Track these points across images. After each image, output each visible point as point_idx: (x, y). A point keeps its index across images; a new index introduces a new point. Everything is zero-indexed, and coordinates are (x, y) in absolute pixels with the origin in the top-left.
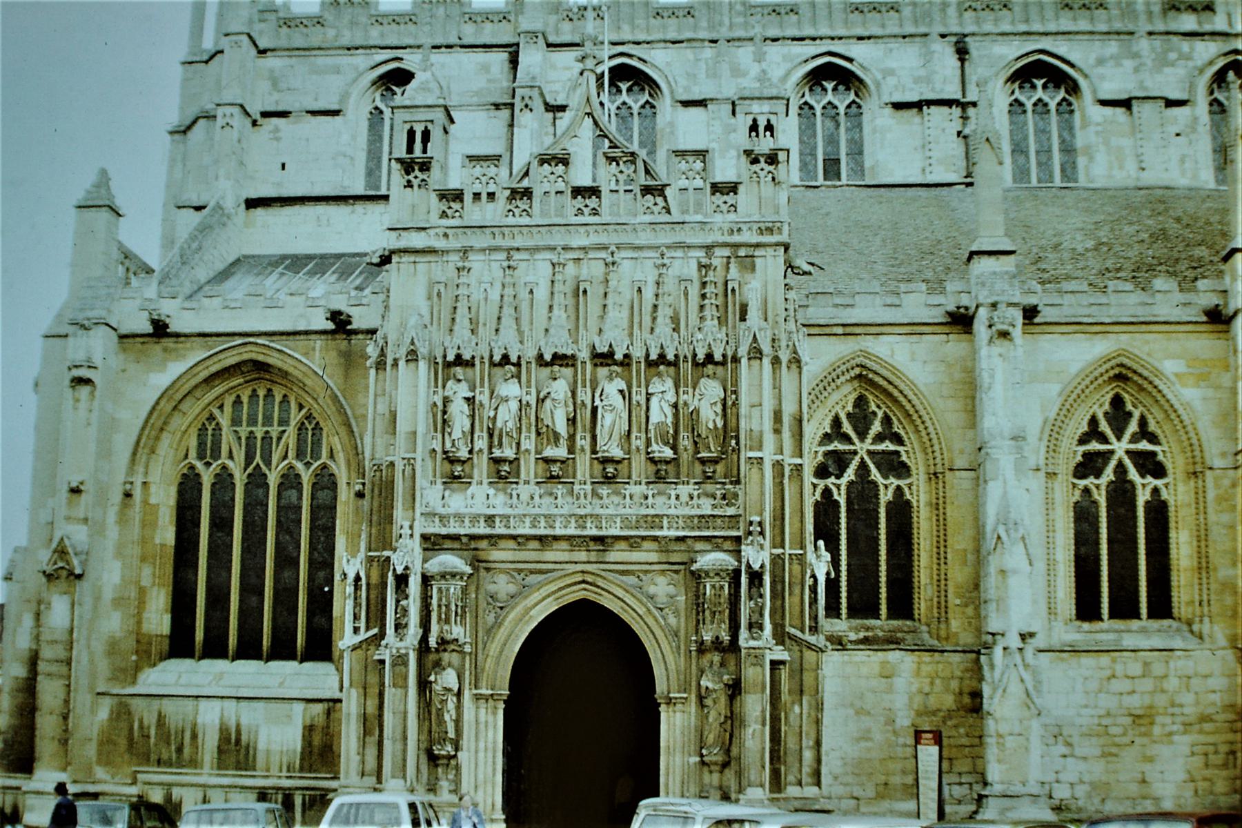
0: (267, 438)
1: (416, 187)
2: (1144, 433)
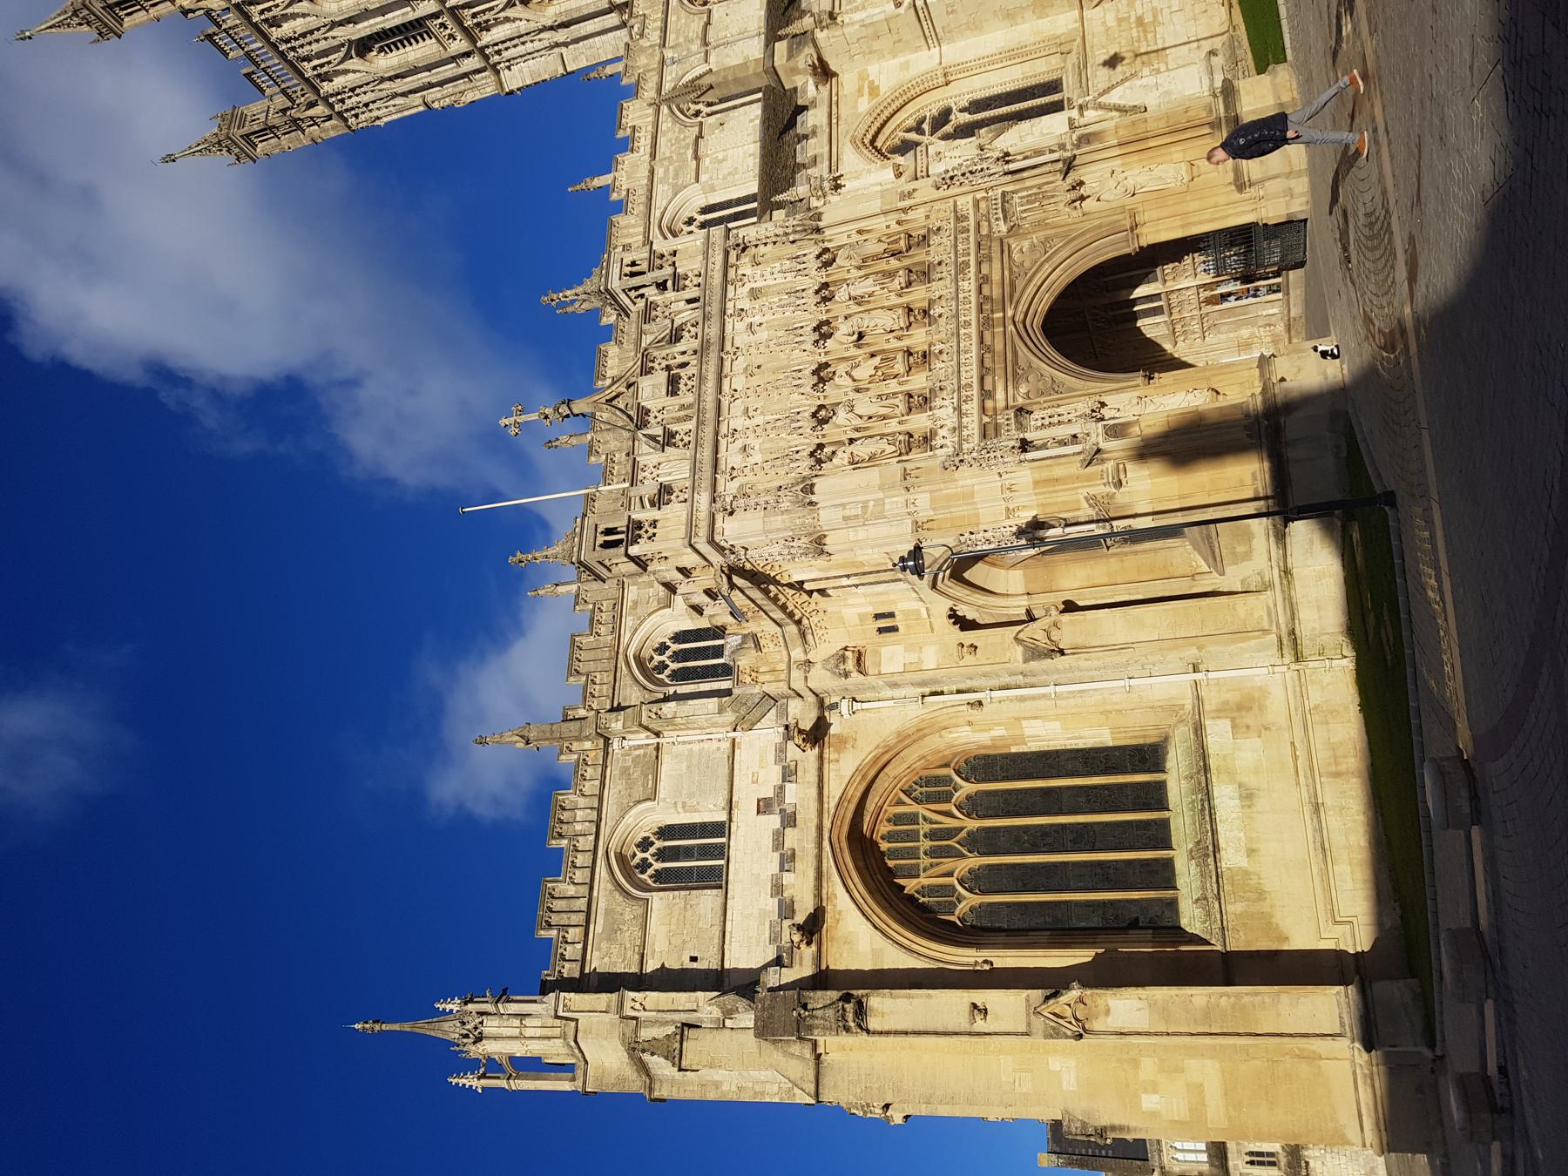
0: (932, 835)
1: (655, 531)
2: (918, 129)
